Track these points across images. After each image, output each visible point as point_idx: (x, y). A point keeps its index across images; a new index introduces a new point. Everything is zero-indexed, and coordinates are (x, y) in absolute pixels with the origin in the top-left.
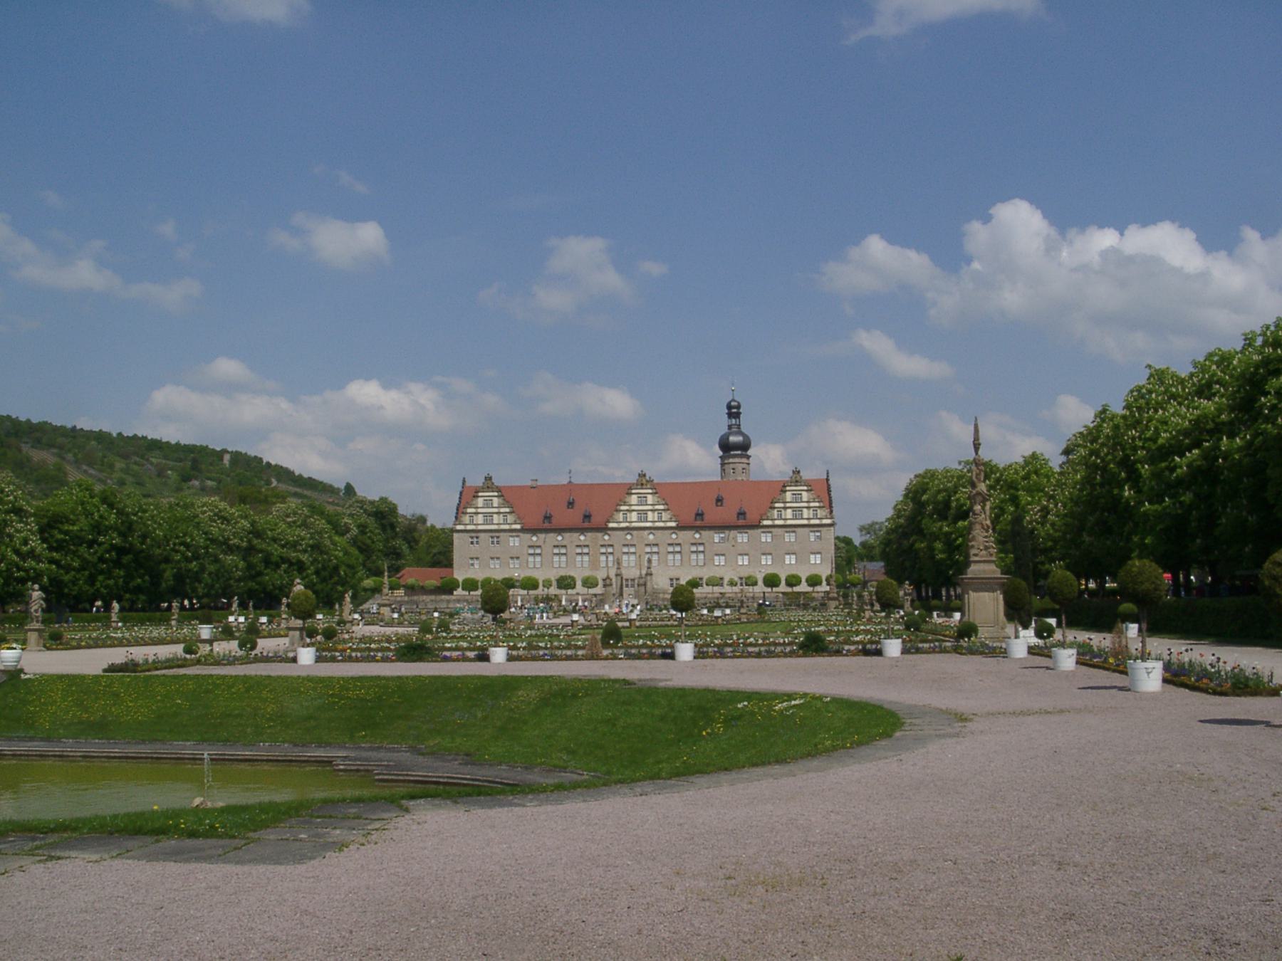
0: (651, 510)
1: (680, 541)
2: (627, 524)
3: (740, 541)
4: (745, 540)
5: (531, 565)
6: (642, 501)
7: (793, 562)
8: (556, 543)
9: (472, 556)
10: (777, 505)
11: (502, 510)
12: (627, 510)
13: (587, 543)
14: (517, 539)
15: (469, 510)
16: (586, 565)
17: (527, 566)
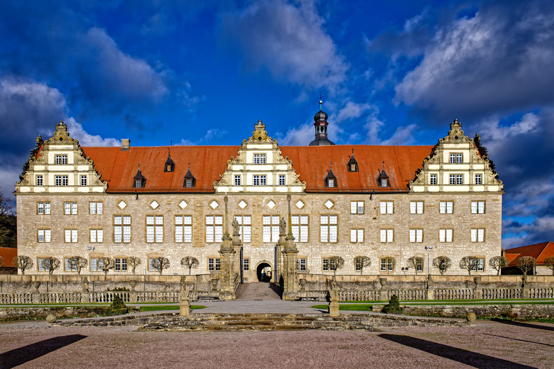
0: (272, 171)
1: (308, 212)
2: (239, 189)
3: (383, 211)
4: (390, 211)
5: (118, 239)
6: (260, 160)
7: (449, 239)
8: (150, 212)
9: (40, 227)
10: (431, 167)
11: (80, 168)
12: (241, 171)
13: (188, 213)
14: (100, 205)
15: (36, 168)
16: (188, 239)
17: (114, 240)
